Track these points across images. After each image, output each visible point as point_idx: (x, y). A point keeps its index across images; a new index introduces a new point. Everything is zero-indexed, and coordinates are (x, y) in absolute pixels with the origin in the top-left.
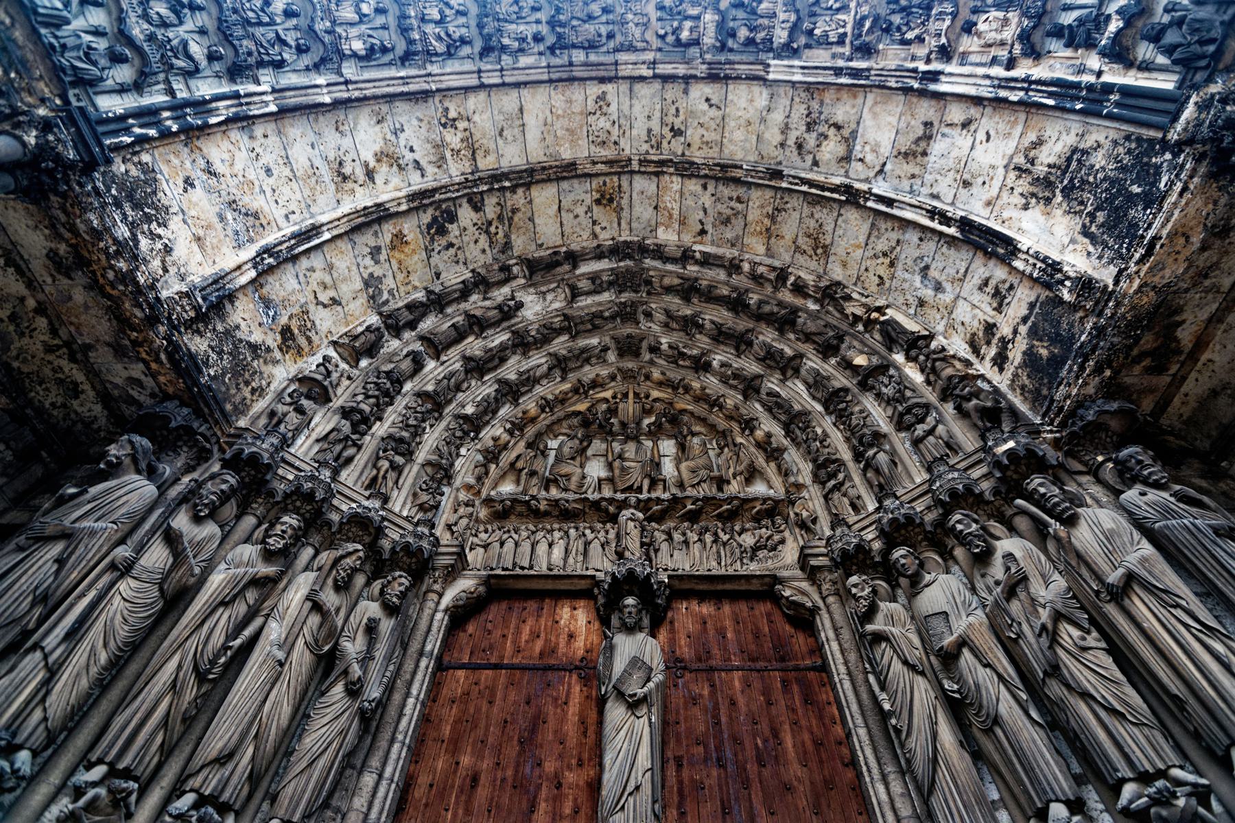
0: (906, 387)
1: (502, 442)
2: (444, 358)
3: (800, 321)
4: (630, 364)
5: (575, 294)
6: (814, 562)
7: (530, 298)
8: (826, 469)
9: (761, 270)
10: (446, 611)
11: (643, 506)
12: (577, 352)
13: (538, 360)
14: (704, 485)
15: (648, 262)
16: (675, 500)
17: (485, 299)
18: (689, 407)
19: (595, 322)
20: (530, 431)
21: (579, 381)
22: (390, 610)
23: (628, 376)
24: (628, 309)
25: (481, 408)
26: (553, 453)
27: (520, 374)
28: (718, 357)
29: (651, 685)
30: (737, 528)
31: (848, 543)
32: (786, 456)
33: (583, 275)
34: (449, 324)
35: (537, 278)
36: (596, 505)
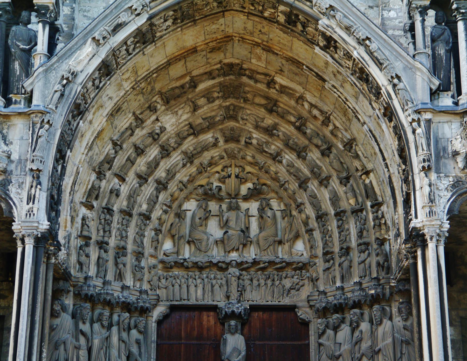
0: (364, 229)
1: (163, 221)
2: (127, 179)
3: (332, 156)
4: (232, 145)
5: (195, 108)
6: (312, 303)
7: (168, 117)
8: (328, 255)
9: (315, 112)
10: (155, 322)
11: (239, 265)
12: (199, 150)
13: (176, 158)
14: (271, 247)
15: (245, 79)
16: (255, 263)
17: (143, 128)
18: (269, 182)
19: (211, 124)
20: (175, 205)
21: (201, 165)
22: (140, 332)
23: (231, 156)
24: (231, 112)
25: (151, 207)
26: (189, 214)
27: (168, 171)
28: (287, 157)
29: (240, 357)
30: (284, 275)
31: (321, 306)
32: (314, 233)
33: (201, 91)
34: (126, 157)
35: (172, 102)
36: (216, 265)
